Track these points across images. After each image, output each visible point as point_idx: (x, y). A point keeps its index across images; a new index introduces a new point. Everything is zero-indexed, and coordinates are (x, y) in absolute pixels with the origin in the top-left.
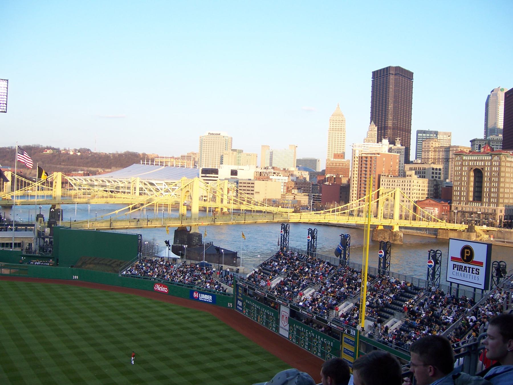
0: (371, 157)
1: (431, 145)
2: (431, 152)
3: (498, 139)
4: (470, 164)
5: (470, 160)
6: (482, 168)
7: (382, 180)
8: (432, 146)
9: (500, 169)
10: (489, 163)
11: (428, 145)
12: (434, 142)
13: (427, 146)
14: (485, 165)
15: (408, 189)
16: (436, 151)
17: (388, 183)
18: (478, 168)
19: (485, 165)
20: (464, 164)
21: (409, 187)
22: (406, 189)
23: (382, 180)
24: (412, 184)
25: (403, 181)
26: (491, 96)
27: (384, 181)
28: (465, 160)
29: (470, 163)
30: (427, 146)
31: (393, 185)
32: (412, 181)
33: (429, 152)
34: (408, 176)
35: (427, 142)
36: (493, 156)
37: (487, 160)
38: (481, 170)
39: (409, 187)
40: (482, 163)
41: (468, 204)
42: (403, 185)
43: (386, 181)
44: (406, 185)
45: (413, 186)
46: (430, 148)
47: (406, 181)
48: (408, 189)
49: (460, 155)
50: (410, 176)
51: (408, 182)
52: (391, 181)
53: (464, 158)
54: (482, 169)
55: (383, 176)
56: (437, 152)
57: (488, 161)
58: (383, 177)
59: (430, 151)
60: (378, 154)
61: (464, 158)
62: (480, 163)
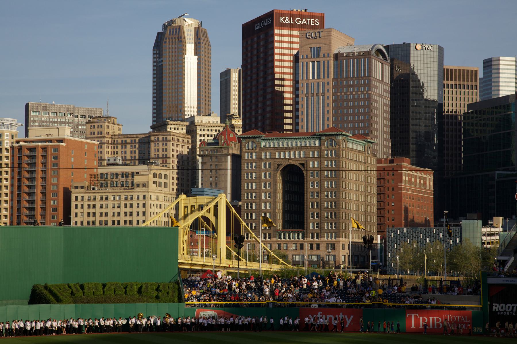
0: (44, 149)
1: (107, 130)
2: (106, 145)
3: (211, 122)
4: (277, 157)
5: (275, 149)
6: (303, 162)
7: (76, 198)
8: (108, 133)
9: (337, 164)
10: (316, 153)
11: (100, 130)
12: (110, 125)
13: (96, 133)
14: (307, 157)
15: (141, 214)
16: (118, 144)
17: (92, 203)
19: (307, 157)
20: (263, 157)
21: (141, 210)
22: (135, 214)
23: (76, 198)
24: (149, 202)
25: (126, 198)
26: (167, 35)
27: (80, 198)
28: (265, 149)
29: (277, 154)
30: (96, 133)
31: (104, 206)
32: (148, 196)
33: (103, 145)
34: (138, 185)
35: (96, 125)
37: (311, 148)
38: (300, 166)
39: (141, 210)
40: (302, 153)
41: (276, 237)
42: (128, 206)
43: (86, 198)
44: (135, 205)
45: (151, 208)
46: (105, 137)
47: (135, 197)
48: (141, 214)
49: (254, 140)
50: (144, 185)
51: (138, 198)
52: (98, 198)
54: (303, 165)
55: (76, 187)
56: (119, 146)
58: (79, 190)
59: (104, 143)
60: (61, 141)
61: (263, 144)
62: (297, 153)
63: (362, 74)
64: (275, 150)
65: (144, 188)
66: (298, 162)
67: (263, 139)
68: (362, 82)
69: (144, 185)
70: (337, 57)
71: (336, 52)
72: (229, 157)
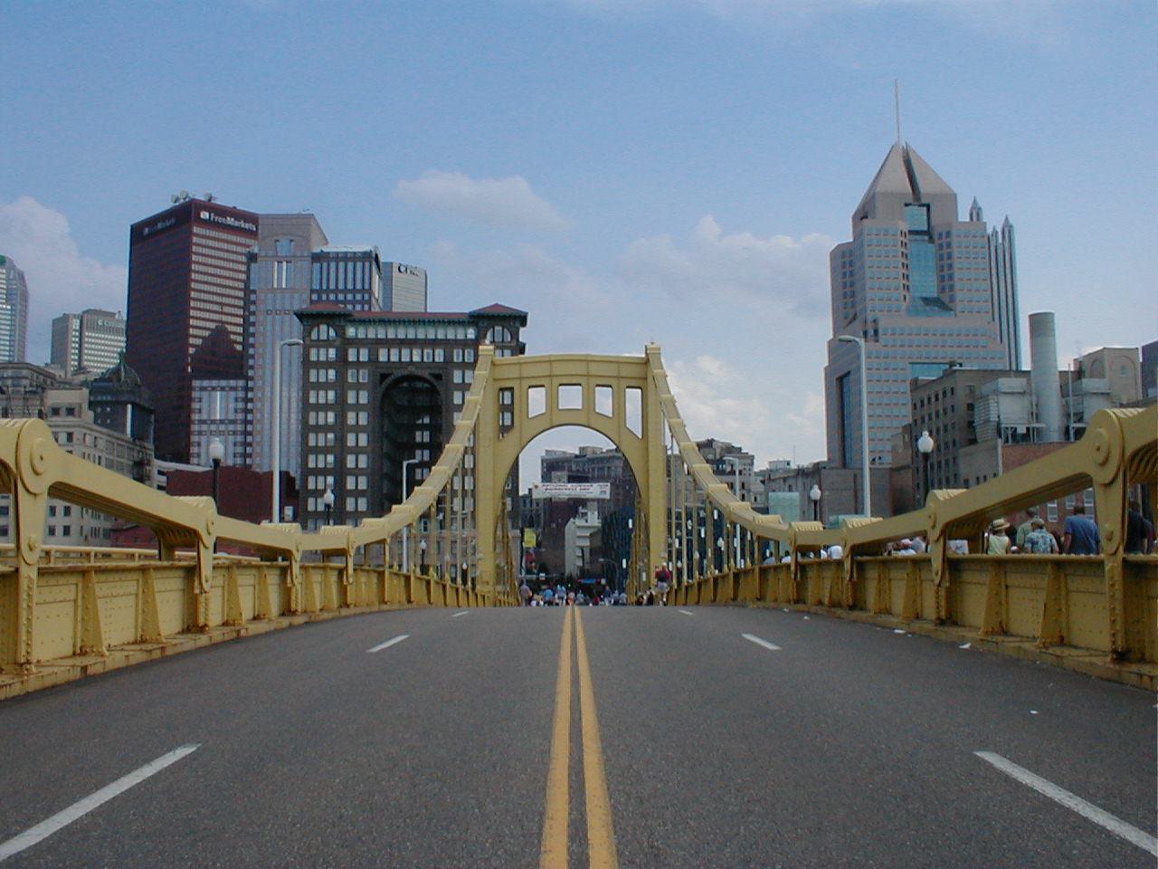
6: (437, 372)
14: (449, 363)
18: (419, 372)
19: (449, 363)
28: (357, 343)
34: (56, 411)
36: (483, 324)
38: (432, 379)
50: (70, 411)
53: (351, 332)
54: (438, 377)
57: (464, 344)
61: (351, 332)
63: (359, 286)
64: (377, 344)
65: (71, 418)
66: (429, 370)
67: (350, 321)
68: (359, 297)
69: (70, 411)
70: (317, 258)
71: (316, 250)
72: (129, 407)
